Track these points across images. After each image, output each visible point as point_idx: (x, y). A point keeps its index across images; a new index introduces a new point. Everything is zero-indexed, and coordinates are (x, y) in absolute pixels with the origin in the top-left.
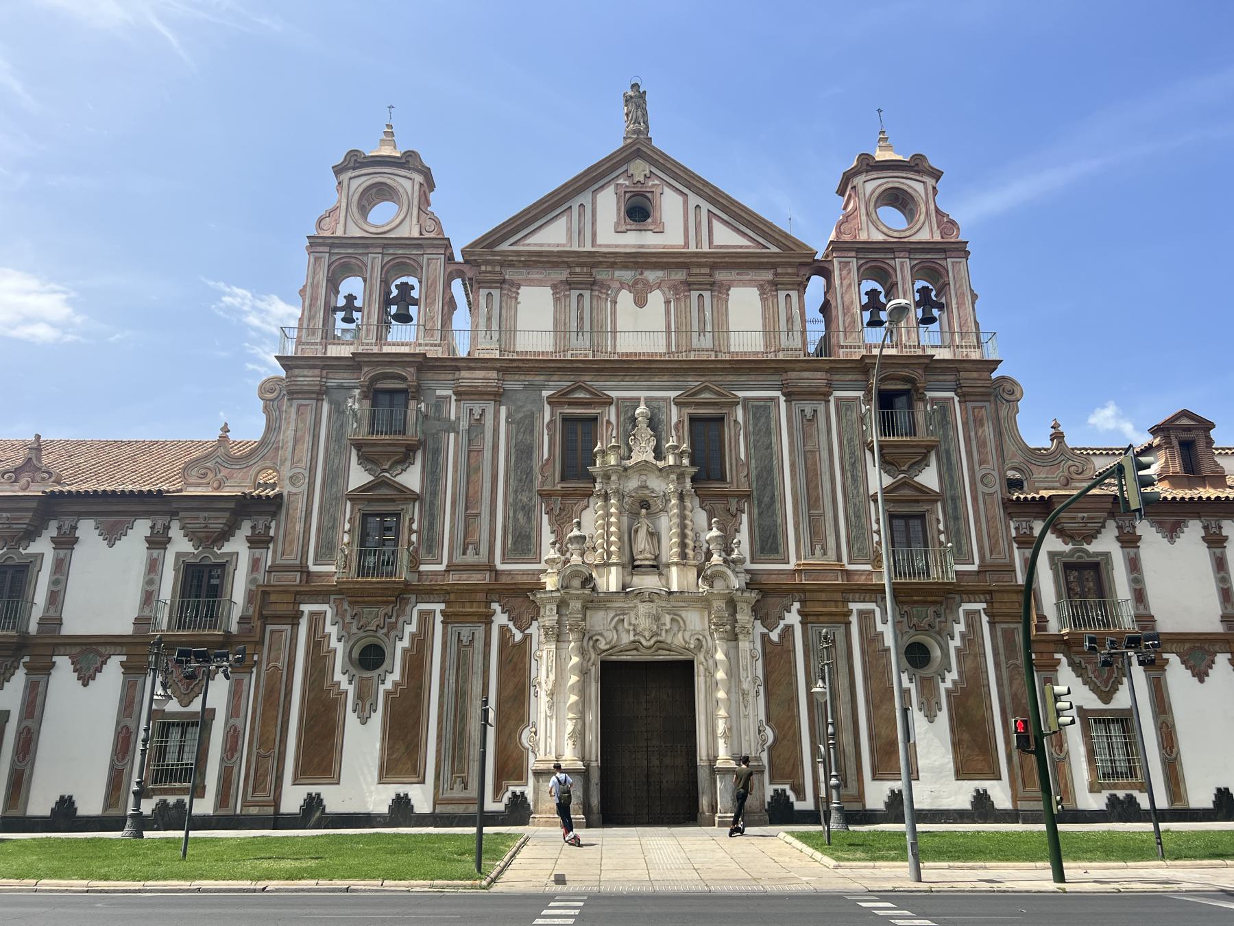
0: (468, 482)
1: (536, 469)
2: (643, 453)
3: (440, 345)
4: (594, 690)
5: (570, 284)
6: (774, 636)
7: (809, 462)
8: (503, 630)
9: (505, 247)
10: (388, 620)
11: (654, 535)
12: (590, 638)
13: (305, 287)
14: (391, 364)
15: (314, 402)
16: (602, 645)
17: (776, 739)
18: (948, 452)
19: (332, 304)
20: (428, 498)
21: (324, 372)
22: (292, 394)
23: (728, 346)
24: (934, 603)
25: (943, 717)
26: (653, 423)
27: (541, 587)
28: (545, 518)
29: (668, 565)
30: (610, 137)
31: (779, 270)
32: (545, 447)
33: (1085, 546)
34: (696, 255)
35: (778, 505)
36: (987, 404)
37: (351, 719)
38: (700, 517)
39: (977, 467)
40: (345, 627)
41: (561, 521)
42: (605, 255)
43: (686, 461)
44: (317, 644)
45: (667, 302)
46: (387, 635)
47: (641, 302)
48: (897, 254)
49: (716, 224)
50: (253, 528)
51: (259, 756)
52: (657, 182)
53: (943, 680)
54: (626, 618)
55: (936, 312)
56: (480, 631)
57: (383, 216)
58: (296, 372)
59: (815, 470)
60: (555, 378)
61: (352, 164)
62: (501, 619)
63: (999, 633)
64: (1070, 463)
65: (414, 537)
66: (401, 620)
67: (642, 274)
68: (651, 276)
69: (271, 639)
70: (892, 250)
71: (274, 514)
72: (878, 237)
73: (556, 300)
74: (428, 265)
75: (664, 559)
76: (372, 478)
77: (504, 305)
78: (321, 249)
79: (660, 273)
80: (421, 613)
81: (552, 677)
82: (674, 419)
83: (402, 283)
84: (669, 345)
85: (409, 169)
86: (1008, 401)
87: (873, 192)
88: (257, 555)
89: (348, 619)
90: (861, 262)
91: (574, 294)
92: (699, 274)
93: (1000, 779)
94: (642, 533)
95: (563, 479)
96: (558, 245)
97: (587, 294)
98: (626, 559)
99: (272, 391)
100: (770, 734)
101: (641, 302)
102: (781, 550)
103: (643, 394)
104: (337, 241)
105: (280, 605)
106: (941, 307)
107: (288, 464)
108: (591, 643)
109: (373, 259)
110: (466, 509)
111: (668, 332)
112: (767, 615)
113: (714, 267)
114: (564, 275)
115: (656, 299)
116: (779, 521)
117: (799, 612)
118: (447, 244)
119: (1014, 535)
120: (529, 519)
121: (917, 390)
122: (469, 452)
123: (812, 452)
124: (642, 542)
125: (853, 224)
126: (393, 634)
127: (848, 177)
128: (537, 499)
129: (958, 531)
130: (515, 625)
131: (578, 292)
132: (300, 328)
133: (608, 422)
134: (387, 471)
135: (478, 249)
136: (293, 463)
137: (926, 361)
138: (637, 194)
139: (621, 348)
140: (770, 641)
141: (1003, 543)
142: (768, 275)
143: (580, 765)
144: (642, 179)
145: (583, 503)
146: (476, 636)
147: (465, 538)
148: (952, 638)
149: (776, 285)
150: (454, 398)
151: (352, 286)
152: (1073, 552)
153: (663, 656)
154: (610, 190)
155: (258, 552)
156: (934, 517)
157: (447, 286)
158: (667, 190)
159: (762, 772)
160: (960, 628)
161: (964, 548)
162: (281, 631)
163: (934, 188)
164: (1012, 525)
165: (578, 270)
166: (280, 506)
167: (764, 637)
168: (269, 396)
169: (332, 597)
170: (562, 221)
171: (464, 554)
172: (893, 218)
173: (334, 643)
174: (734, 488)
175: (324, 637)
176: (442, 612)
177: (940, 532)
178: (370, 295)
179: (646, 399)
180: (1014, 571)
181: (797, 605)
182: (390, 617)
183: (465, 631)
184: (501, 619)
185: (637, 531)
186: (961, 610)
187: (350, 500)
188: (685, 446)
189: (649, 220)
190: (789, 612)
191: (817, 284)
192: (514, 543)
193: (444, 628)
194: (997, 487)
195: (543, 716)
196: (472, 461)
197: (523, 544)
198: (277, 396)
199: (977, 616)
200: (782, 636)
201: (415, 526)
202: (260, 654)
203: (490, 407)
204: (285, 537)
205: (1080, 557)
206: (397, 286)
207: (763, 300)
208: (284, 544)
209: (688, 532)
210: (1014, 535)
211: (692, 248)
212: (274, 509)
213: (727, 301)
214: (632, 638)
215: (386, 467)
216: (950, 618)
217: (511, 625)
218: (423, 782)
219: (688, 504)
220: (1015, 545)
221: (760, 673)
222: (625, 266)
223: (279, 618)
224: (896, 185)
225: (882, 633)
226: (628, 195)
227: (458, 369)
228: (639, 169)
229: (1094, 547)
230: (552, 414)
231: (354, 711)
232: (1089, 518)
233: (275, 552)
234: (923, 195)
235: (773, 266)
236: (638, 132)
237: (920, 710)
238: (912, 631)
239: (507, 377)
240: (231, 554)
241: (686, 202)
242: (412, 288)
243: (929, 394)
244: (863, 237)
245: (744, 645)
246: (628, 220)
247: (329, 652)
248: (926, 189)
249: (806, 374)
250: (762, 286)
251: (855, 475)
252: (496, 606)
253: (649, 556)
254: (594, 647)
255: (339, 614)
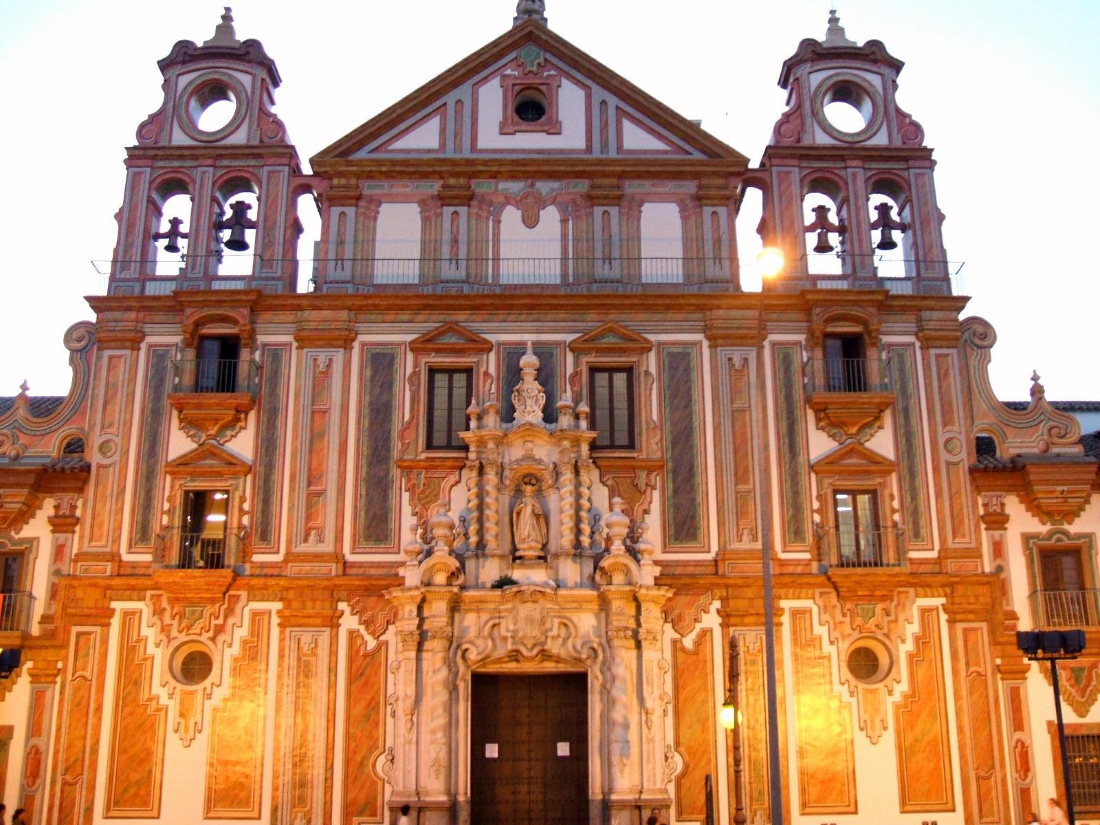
0: (311, 451)
1: (395, 435)
2: (530, 411)
3: (279, 279)
4: (464, 710)
5: (443, 199)
6: (688, 642)
7: (737, 428)
8: (353, 635)
9: (362, 154)
10: (214, 622)
11: (543, 517)
12: (459, 646)
13: (121, 210)
14: (220, 303)
15: (128, 352)
16: (473, 655)
17: (686, 766)
18: (906, 410)
19: (153, 232)
20: (262, 471)
21: (141, 315)
22: (102, 344)
23: (640, 277)
24: (884, 598)
25: (889, 740)
26: (545, 377)
27: (399, 582)
28: (406, 496)
29: (556, 556)
30: (496, 16)
31: (705, 181)
32: (405, 405)
33: (1066, 527)
34: (600, 162)
35: (698, 479)
36: (954, 351)
37: (173, 743)
38: (600, 495)
39: (940, 428)
40: (165, 629)
41: (425, 499)
42: (486, 163)
43: (584, 424)
44: (130, 649)
45: (564, 221)
46: (213, 639)
47: (531, 221)
48: (850, 163)
49: (627, 124)
50: (57, 507)
51: (65, 783)
52: (553, 72)
53: (890, 693)
54: (503, 622)
55: (897, 235)
56: (325, 636)
57: (216, 117)
58: (109, 315)
59: (744, 434)
60: (421, 317)
61: (180, 59)
62: (349, 622)
63: (960, 635)
64: (1051, 423)
65: (246, 520)
66: (230, 621)
67: (532, 185)
68: (545, 187)
69: (77, 643)
70: (842, 158)
71: (81, 490)
72: (822, 139)
73: (425, 220)
74: (269, 178)
75: (553, 547)
76: (195, 446)
77: (360, 226)
78: (142, 162)
79: (556, 185)
80: (255, 615)
81: (411, 691)
82: (570, 370)
83: (238, 203)
84: (564, 276)
85: (249, 62)
86: (980, 347)
87: (820, 86)
88: (61, 541)
89: (167, 620)
90: (805, 172)
91: (448, 211)
92: (602, 184)
93: (953, 810)
94: (527, 512)
95: (430, 446)
96: (429, 151)
97: (463, 211)
98: (507, 547)
99: (80, 340)
100: (678, 762)
101: (531, 221)
102: (701, 533)
103: (530, 338)
104: (160, 152)
105: (88, 598)
106: (903, 228)
107: (98, 428)
108: (459, 654)
109: (204, 173)
110: (309, 485)
111: (564, 259)
112: (680, 617)
113: (622, 176)
114: (435, 187)
115: (550, 216)
116: (699, 499)
117: (718, 611)
118: (290, 153)
119: (981, 511)
120: (385, 496)
121: (869, 333)
122: (313, 412)
123: (743, 411)
124: (526, 525)
125: (796, 121)
126: (221, 638)
127: (790, 67)
128: (396, 473)
129: (915, 512)
130: (367, 629)
131: (452, 209)
132: (115, 262)
133: (486, 374)
134: (214, 437)
135: (328, 159)
136: (103, 428)
137: (880, 297)
138: (529, 87)
139: (504, 281)
140: (683, 650)
141: (968, 524)
142: (690, 187)
143: (443, 798)
144: (534, 69)
145: (453, 478)
146: (320, 641)
147: (307, 523)
148: (903, 641)
149: (699, 199)
150: (295, 344)
151: (178, 207)
152: (1051, 534)
153: (550, 667)
154: (495, 83)
155: (62, 537)
156: (887, 492)
157: (293, 205)
158: (565, 83)
159: (668, 807)
160: (913, 628)
161: (923, 532)
162: (89, 633)
163: (894, 82)
164: (980, 501)
165: (452, 181)
166: (86, 481)
167: (675, 643)
168: (80, 345)
169: (149, 593)
170: (434, 124)
171: (306, 540)
172: (846, 118)
173: (151, 649)
174: (644, 456)
175: (139, 641)
176: (279, 612)
177: (894, 511)
178: (198, 219)
179: (535, 344)
180: (980, 556)
181: (717, 604)
182: (217, 618)
183: (306, 638)
184: (349, 622)
185: (519, 514)
186: (915, 607)
187: (172, 473)
188: (584, 408)
189: (543, 119)
190: (708, 612)
191: (753, 199)
192: (368, 527)
193: (282, 633)
194: (964, 455)
195: (402, 740)
196: (317, 424)
197: (377, 526)
198: (84, 344)
199: (934, 613)
200: (699, 642)
201: (246, 506)
202: (65, 659)
203: (339, 356)
204: (93, 519)
205: (1059, 540)
206: (232, 206)
207: (685, 218)
208: (92, 527)
209: (584, 514)
210: (981, 511)
211: (597, 154)
212: (80, 484)
213: (639, 220)
214: (510, 646)
215: (212, 432)
216: (901, 618)
217: (362, 629)
218: (259, 818)
219: (584, 477)
220: (983, 526)
221: (669, 688)
222: (513, 176)
223: (85, 619)
224: (847, 78)
225: (820, 639)
226: (517, 88)
227: (300, 308)
228: (532, 55)
229: (1077, 527)
230: (416, 365)
231: (176, 731)
232: (1069, 492)
233: (81, 538)
234: (880, 89)
235: (696, 176)
236: (529, 12)
237: (861, 729)
238: (856, 635)
239: (362, 317)
240: (32, 541)
241: (589, 97)
242: (249, 207)
243: (886, 339)
244: (806, 141)
245: (649, 654)
246: (516, 118)
247: (145, 659)
248: (884, 83)
249: (733, 313)
250: (682, 200)
251: (791, 442)
252: (342, 606)
253: (534, 544)
254: (464, 657)
255: (158, 612)
